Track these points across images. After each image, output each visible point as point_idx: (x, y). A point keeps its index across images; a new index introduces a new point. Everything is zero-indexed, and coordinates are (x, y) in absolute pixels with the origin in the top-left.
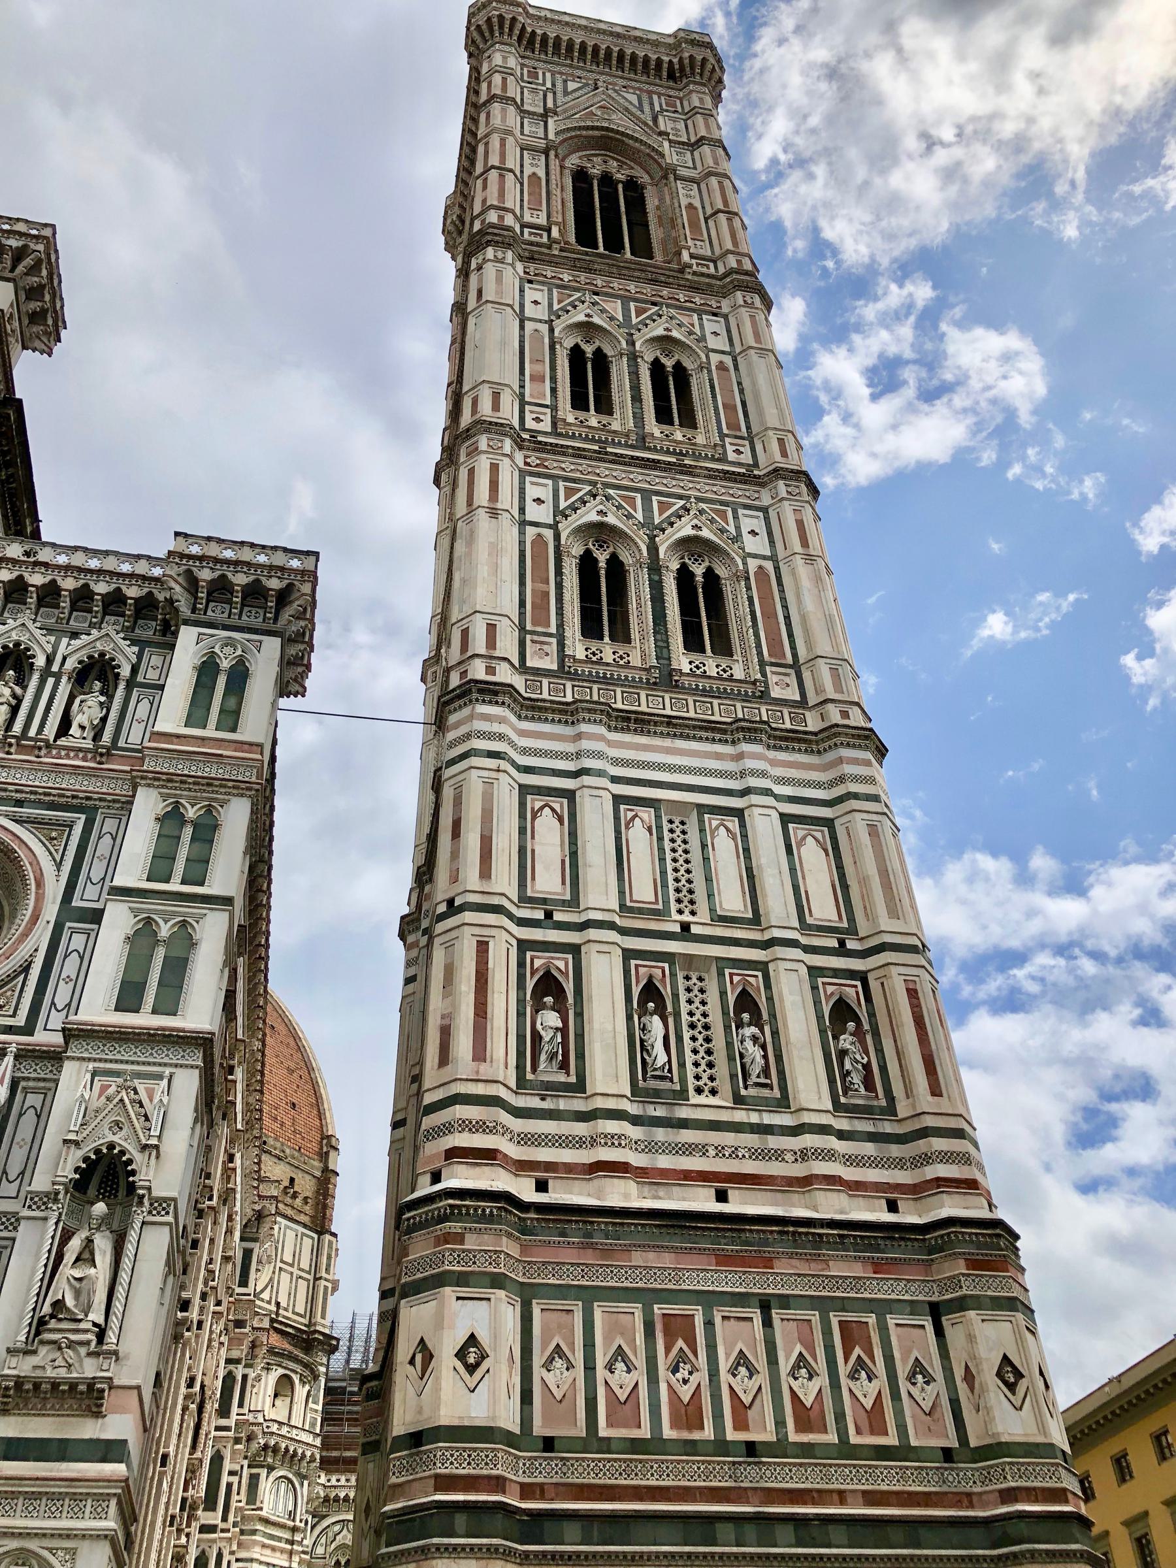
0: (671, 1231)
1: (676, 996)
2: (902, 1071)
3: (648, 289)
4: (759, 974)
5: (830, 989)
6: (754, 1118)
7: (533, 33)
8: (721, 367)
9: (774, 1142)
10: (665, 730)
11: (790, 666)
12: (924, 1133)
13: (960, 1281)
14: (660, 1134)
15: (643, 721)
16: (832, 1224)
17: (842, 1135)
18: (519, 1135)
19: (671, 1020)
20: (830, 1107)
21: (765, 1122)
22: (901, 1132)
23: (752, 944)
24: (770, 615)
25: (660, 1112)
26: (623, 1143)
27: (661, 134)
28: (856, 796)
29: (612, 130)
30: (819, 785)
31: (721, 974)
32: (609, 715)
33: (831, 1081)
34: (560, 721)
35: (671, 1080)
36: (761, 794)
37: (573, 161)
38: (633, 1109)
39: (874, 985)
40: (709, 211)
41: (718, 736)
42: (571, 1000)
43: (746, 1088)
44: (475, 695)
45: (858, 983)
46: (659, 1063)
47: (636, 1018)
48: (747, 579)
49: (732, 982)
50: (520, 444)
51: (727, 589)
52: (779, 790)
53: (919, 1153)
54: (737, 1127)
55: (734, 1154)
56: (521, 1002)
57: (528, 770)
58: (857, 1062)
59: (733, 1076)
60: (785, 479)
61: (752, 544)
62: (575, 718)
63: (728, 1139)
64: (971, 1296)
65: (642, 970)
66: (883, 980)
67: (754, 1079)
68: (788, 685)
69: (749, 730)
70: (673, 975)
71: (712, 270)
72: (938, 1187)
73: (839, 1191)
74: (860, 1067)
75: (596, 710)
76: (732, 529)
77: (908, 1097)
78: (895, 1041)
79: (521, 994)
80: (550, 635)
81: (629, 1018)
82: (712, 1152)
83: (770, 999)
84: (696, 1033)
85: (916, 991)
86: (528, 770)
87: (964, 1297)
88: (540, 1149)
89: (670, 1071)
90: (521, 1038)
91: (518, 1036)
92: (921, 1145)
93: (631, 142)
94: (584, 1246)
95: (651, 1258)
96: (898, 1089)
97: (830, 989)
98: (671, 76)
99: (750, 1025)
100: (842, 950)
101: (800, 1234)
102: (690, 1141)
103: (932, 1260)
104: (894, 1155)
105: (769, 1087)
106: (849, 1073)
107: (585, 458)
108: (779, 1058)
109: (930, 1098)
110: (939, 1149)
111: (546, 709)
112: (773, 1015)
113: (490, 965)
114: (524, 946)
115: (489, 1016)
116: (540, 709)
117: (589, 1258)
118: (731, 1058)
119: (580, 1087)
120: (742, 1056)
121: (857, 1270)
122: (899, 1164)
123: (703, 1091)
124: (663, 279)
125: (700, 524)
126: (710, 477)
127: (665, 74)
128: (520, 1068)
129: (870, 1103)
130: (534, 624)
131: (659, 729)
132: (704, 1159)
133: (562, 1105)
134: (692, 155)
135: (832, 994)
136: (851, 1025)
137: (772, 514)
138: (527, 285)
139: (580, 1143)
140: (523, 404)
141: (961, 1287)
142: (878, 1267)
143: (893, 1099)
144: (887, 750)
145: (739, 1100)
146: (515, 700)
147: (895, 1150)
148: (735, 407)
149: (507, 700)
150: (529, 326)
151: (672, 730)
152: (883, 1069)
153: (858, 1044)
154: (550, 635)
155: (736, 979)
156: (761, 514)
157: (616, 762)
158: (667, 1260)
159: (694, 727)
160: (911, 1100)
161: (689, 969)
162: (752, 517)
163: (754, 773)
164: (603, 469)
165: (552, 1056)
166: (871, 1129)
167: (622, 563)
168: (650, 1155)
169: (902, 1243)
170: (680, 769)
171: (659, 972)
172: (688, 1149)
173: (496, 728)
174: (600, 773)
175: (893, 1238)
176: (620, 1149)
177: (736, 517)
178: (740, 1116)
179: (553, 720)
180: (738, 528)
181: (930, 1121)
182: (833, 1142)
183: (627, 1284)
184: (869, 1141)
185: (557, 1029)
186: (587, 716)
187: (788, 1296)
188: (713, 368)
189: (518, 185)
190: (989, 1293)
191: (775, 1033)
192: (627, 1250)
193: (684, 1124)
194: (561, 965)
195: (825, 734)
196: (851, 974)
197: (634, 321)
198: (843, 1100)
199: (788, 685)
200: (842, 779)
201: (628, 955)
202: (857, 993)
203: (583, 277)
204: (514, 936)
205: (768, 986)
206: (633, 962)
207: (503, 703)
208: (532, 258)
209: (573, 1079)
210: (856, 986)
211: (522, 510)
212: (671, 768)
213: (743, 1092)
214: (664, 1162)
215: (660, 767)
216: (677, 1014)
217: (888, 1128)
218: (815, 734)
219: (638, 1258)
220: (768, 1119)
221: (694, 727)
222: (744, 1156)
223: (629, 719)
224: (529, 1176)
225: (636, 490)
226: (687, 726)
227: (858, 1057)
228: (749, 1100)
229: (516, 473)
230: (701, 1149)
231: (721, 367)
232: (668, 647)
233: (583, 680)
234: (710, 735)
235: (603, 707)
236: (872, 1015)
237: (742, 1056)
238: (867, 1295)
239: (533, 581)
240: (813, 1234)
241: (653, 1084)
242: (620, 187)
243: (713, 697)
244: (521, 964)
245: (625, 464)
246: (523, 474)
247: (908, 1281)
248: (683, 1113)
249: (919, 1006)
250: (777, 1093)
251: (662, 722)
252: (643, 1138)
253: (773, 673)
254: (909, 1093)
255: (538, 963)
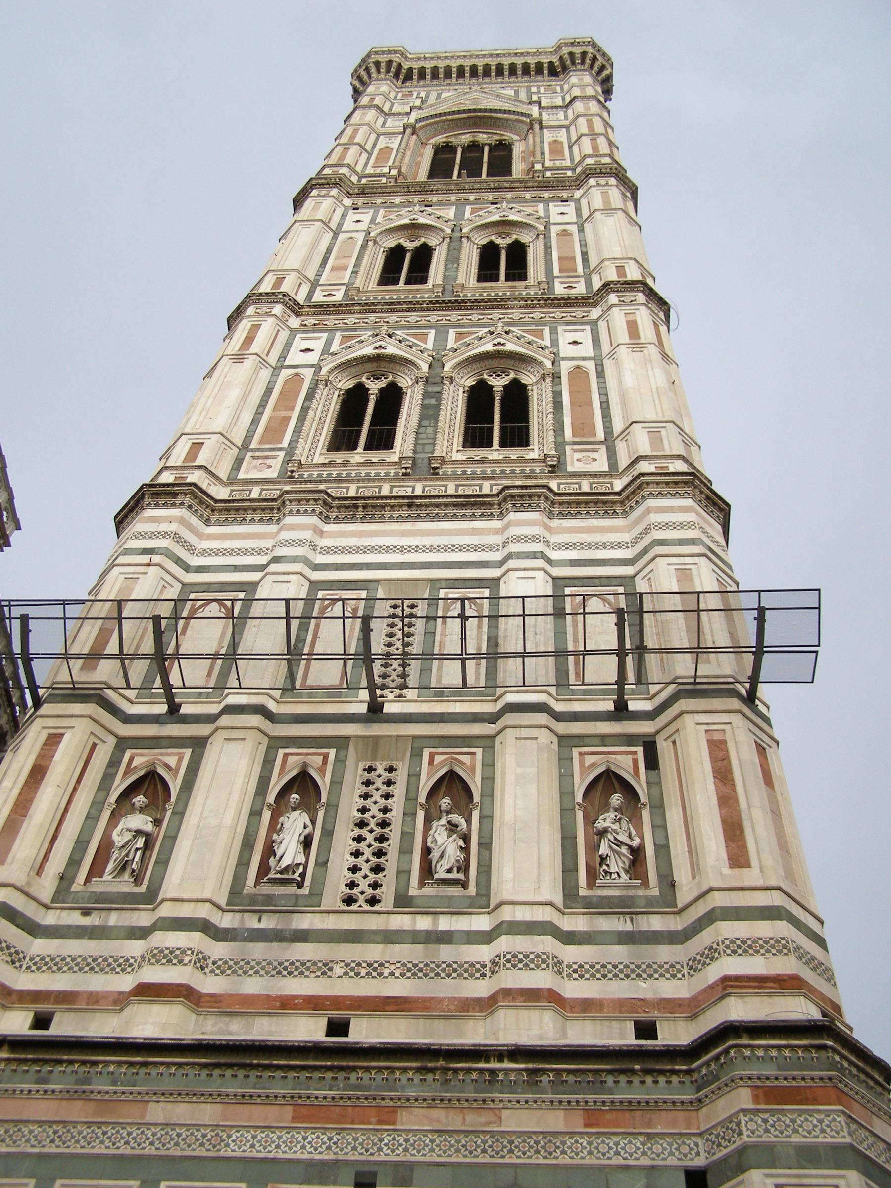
0: (229, 1073)
1: (337, 783)
2: (689, 846)
3: (490, 196)
4: (479, 752)
5: (589, 760)
6: (424, 923)
7: (410, 70)
8: (565, 233)
9: (446, 953)
10: (405, 513)
11: (601, 442)
12: (711, 917)
13: (738, 1124)
14: (258, 951)
15: (374, 507)
16: (516, 1053)
17: (569, 938)
18: (31, 959)
19: (321, 814)
20: (558, 900)
21: (441, 928)
22: (680, 928)
23: (476, 718)
24: (581, 402)
25: (268, 923)
26: (186, 959)
27: (530, 103)
28: (663, 542)
29: (480, 110)
30: (619, 545)
31: (417, 754)
32: (325, 503)
33: (569, 870)
34: (261, 520)
35: (300, 885)
36: (527, 558)
37: (440, 139)
38: (226, 921)
39: (663, 747)
40: (574, 138)
41: (478, 512)
42: (173, 798)
43: (422, 884)
44: (146, 501)
45: (640, 750)
46: (285, 863)
47: (267, 815)
48: (556, 377)
49: (431, 762)
50: (296, 309)
51: (534, 395)
52: (554, 555)
53: (700, 949)
54: (390, 937)
55: (375, 969)
56: (97, 806)
57: (200, 569)
58: (619, 843)
59: (403, 873)
60: (617, 291)
61: (566, 350)
62: (281, 515)
63: (374, 952)
64: (755, 1146)
65: (291, 760)
66: (676, 736)
67: (441, 874)
68: (595, 460)
69: (522, 496)
70: (340, 761)
71: (569, 173)
72: (724, 988)
73: (543, 1008)
74: (624, 850)
75: (308, 500)
76: (547, 342)
77: (694, 877)
78: (684, 809)
79: (102, 795)
80: (280, 449)
81: (255, 814)
82: (338, 970)
83: (489, 780)
84: (364, 832)
85: (724, 742)
86: (200, 569)
87: (743, 1150)
88: (58, 976)
89: (303, 875)
90: (81, 844)
91: (78, 842)
92: (706, 937)
93: (500, 115)
94: (70, 1096)
95: (181, 1111)
96: (681, 873)
97: (589, 760)
98: (553, 72)
99: (448, 813)
100: (621, 711)
101: (456, 1071)
102: (306, 958)
103: (700, 1101)
104: (660, 960)
105: (465, 885)
106: (603, 859)
107: (374, 312)
108: (486, 845)
109: (726, 871)
110: (732, 936)
111: (245, 510)
112: (489, 793)
113: (57, 757)
114: (123, 743)
115: (30, 812)
116: (237, 510)
117: (76, 1111)
118: (406, 850)
119: (151, 897)
120: (426, 851)
121: (556, 1120)
122: (672, 971)
123: (356, 901)
124: (507, 185)
125: (502, 341)
126: (526, 307)
127: (546, 72)
128: (66, 878)
129: (631, 892)
130: (260, 443)
131: (396, 514)
132: (323, 980)
133: (113, 919)
134: (565, 112)
135: (593, 765)
136: (616, 799)
137: (602, 325)
138: (351, 212)
139: (125, 965)
140: (315, 284)
141: (740, 1133)
142: (592, 1116)
143: (673, 884)
144: (728, 506)
145: (403, 901)
146: (201, 502)
147: (665, 953)
148: (573, 259)
149: (187, 500)
150: (342, 237)
151: (414, 512)
152: (662, 849)
153: (624, 823)
154: (280, 449)
155: (438, 759)
156: (588, 328)
157: (327, 551)
158: (208, 1113)
159: (446, 505)
160: (698, 878)
161: (374, 759)
162: (575, 331)
163: (518, 539)
164: (393, 318)
165: (123, 867)
166: (629, 927)
167: (401, 388)
168: (234, 978)
169: (649, 1079)
170: (417, 549)
171: (320, 759)
172: (302, 969)
173: (164, 527)
174: (294, 560)
175: (633, 1072)
176: (179, 968)
177: (554, 332)
178: (401, 921)
179: (253, 520)
180: (555, 342)
181: (719, 900)
182: (547, 944)
183: (126, 1151)
184: (620, 943)
185: (138, 832)
186: (295, 507)
187: (410, 1166)
188: (553, 235)
189: (365, 156)
190: (795, 1139)
191: (487, 818)
192: (143, 1100)
193: (302, 936)
194: (172, 761)
195: (630, 489)
196: (629, 739)
197: (467, 215)
198: (582, 892)
199: (595, 460)
200: (647, 530)
201: (276, 743)
202: (635, 762)
203: (417, 199)
204: (112, 733)
205: (489, 765)
206: (281, 752)
207: (182, 504)
208: (363, 193)
209: (143, 889)
210: (635, 753)
211: (283, 357)
212: (402, 549)
213: (413, 891)
214: (252, 986)
215: (387, 549)
216: (333, 807)
217: (656, 923)
218: (619, 494)
219: (157, 1112)
220: (445, 923)
221: (446, 505)
222: (392, 974)
223: (356, 507)
224: (27, 1009)
225: (431, 327)
226: (437, 506)
227: (623, 838)
228: (418, 902)
229: (284, 335)
230: (325, 969)
231: (565, 233)
232: (434, 444)
233: (306, 482)
234: (468, 512)
235: (316, 495)
236: (655, 784)
237: (426, 851)
238: (564, 1160)
239: (275, 409)
240: (481, 1071)
241: (266, 889)
242: (486, 149)
243: (483, 478)
244: (114, 763)
245: (423, 310)
246: (293, 332)
247: (648, 1135)
248: (304, 922)
249: (726, 758)
250: (472, 890)
251: (401, 506)
252: (226, 957)
253: (576, 451)
254: (695, 869)
255: (137, 762)
